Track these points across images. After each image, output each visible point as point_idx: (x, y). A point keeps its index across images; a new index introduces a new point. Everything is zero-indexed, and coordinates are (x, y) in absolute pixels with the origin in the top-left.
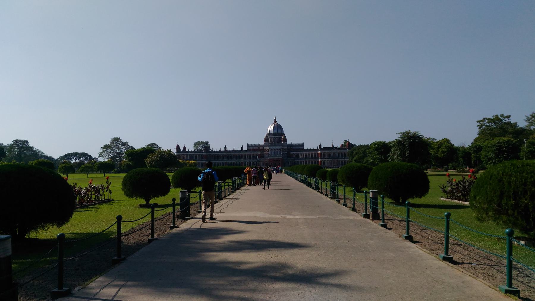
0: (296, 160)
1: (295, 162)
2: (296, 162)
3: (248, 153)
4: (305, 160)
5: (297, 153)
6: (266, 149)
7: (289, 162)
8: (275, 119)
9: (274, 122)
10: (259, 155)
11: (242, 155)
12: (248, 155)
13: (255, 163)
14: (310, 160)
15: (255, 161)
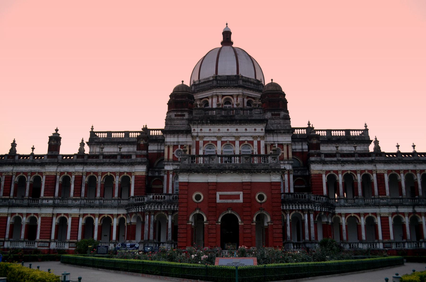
0: (343, 211)
1: (337, 221)
2: (343, 221)
3: (79, 169)
4: (394, 210)
5: (343, 172)
6: (175, 147)
7: (312, 216)
8: (227, 35)
9: (221, 46)
10: (137, 178)
11: (52, 180)
12: (79, 179)
13: (115, 222)
14: (418, 210)
15: (115, 212)
